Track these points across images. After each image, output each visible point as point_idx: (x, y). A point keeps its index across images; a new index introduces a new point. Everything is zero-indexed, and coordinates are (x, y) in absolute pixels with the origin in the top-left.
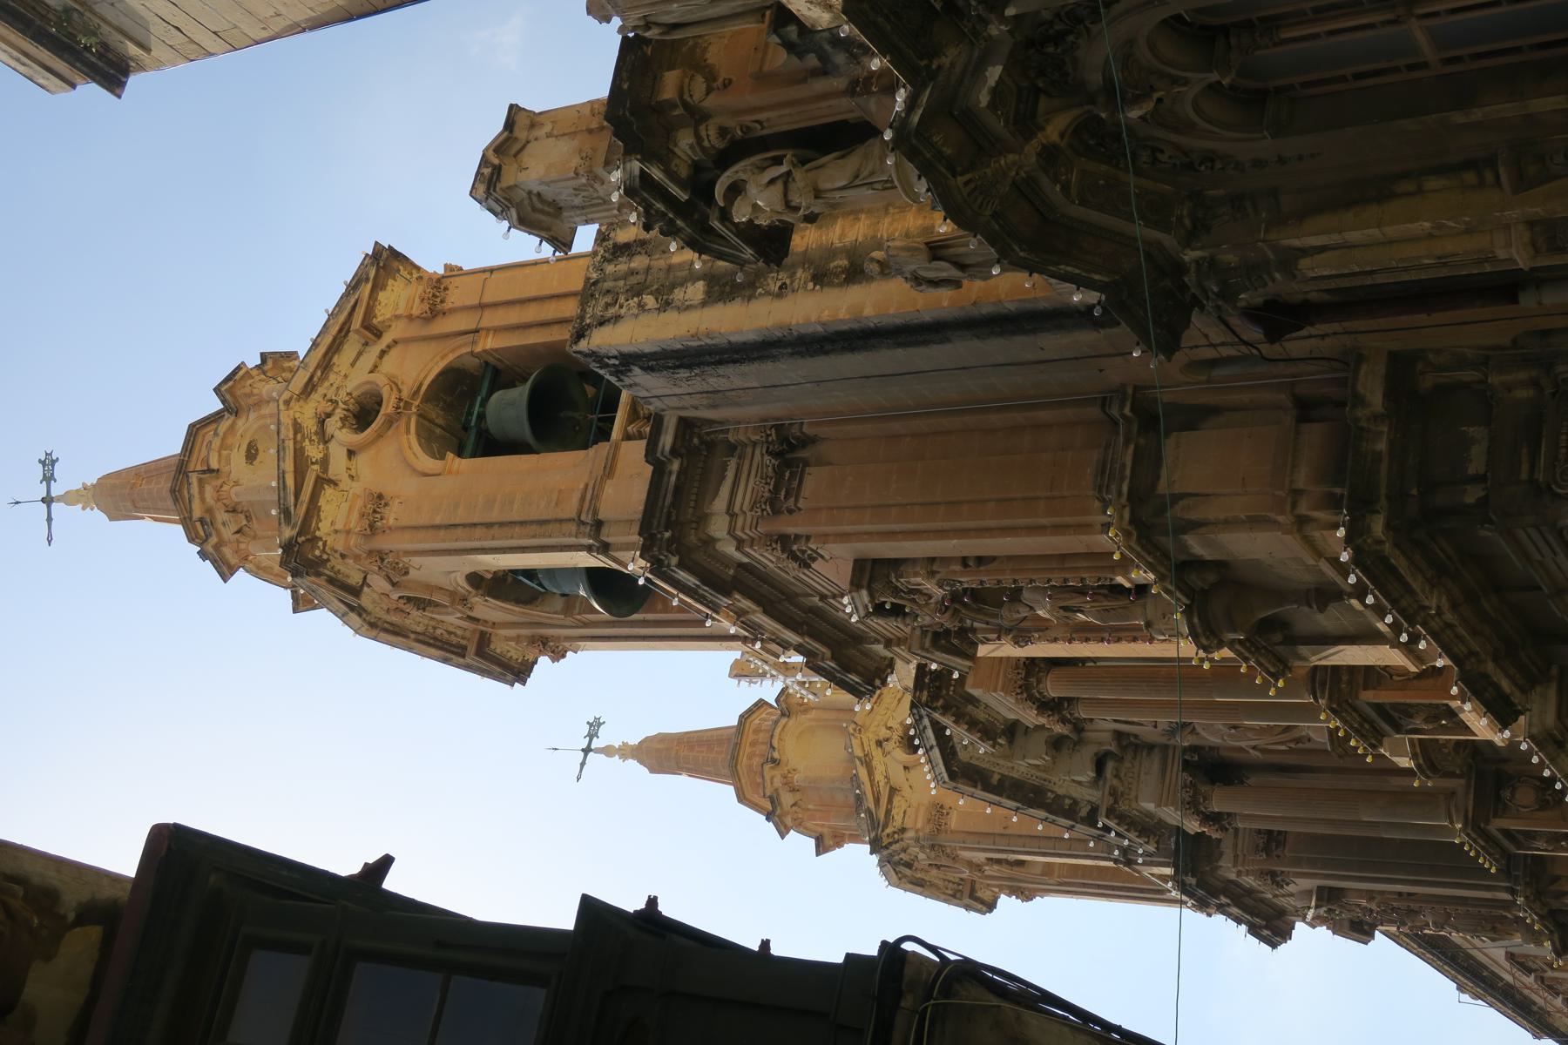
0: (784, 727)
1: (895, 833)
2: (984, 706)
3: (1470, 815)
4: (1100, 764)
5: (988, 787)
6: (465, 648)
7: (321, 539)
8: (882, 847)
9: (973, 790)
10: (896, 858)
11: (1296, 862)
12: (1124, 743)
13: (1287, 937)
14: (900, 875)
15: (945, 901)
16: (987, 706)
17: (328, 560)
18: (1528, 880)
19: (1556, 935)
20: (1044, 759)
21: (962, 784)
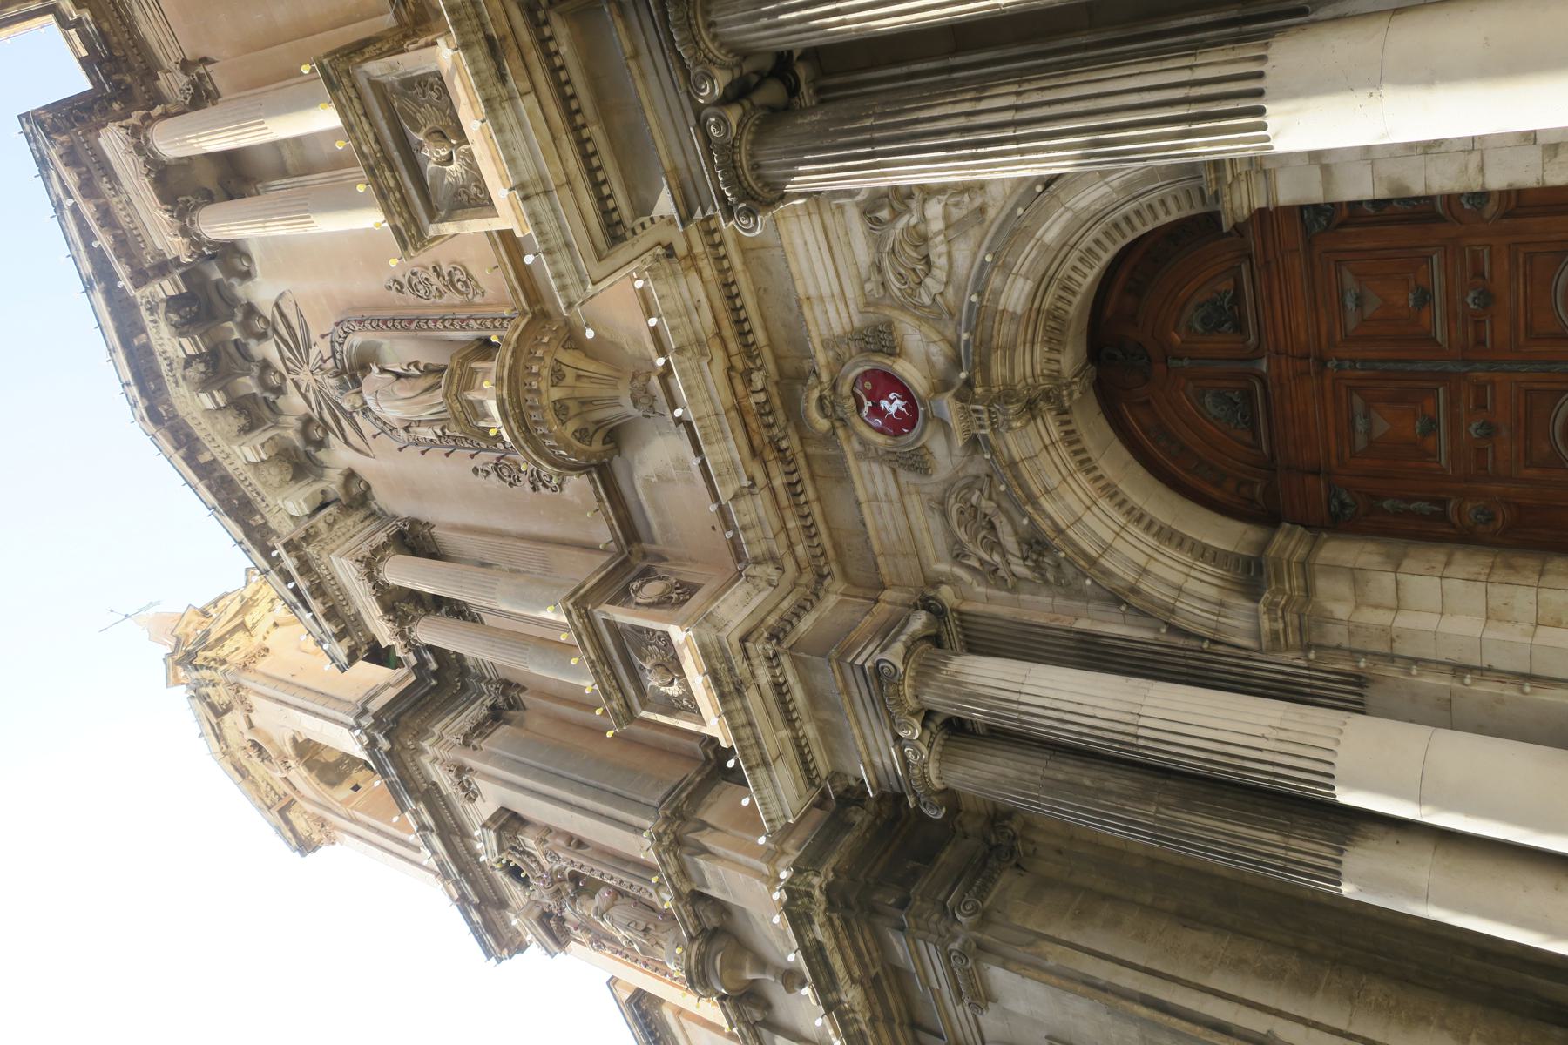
1: (214, 660)
5: (191, 459)
9: (172, 450)
10: (203, 690)
11: (487, 757)
12: (354, 491)
13: (505, 952)
15: (259, 808)
16: (129, 202)
18: (668, 812)
19: (695, 947)
20: (259, 454)
21: (164, 436)
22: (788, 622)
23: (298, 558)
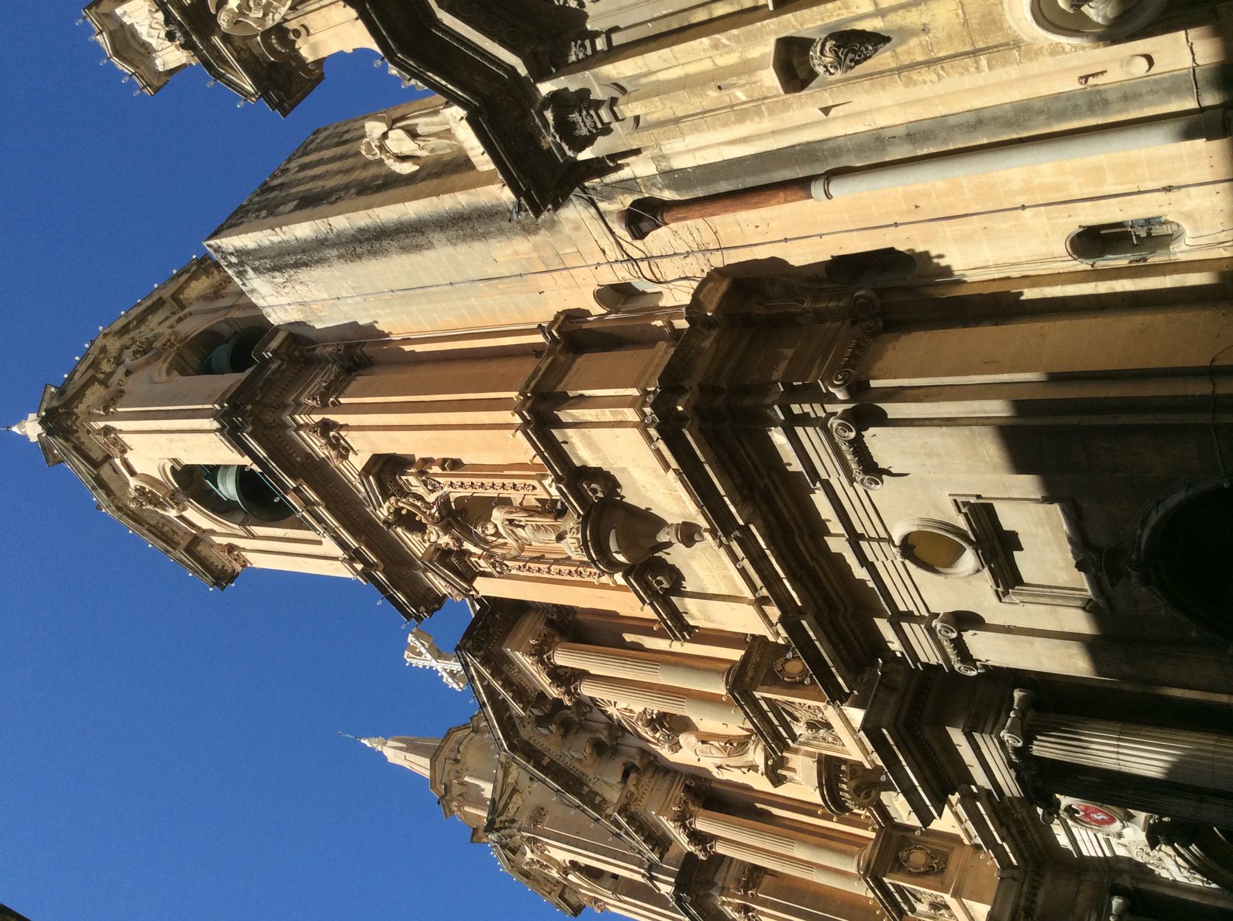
0: (470, 740)
1: (506, 821)
2: (517, 670)
3: (872, 866)
4: (626, 776)
6: (178, 544)
7: (76, 414)
8: (495, 829)
14: (513, 864)
17: (77, 431)
22: (1031, 900)
23: (626, 816)
